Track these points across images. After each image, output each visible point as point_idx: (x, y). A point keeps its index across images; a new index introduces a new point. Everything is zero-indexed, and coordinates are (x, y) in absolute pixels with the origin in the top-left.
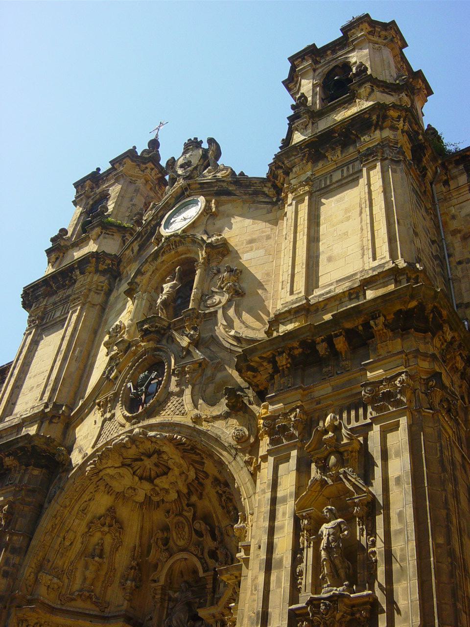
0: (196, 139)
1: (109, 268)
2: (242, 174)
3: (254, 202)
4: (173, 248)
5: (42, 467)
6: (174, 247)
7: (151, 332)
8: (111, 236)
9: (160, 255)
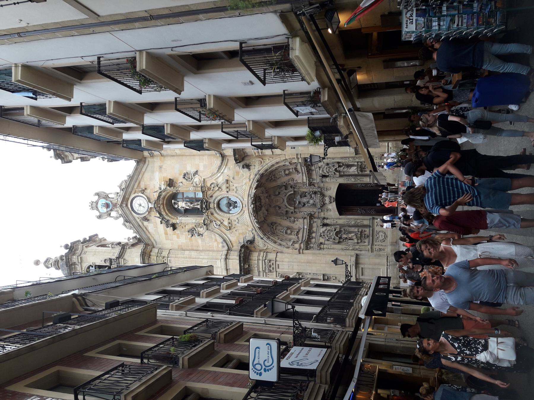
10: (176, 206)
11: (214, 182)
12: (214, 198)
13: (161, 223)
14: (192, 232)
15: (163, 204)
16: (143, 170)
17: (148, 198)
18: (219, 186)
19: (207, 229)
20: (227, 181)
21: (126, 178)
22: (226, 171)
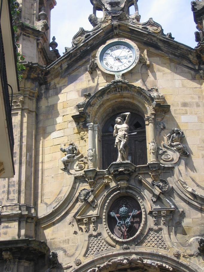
1: (38, 77)
3: (179, 64)
4: (119, 92)
5: (30, 260)
6: (120, 90)
7: (124, 174)
8: (28, 38)
10: (118, 120)
21: (165, 33)
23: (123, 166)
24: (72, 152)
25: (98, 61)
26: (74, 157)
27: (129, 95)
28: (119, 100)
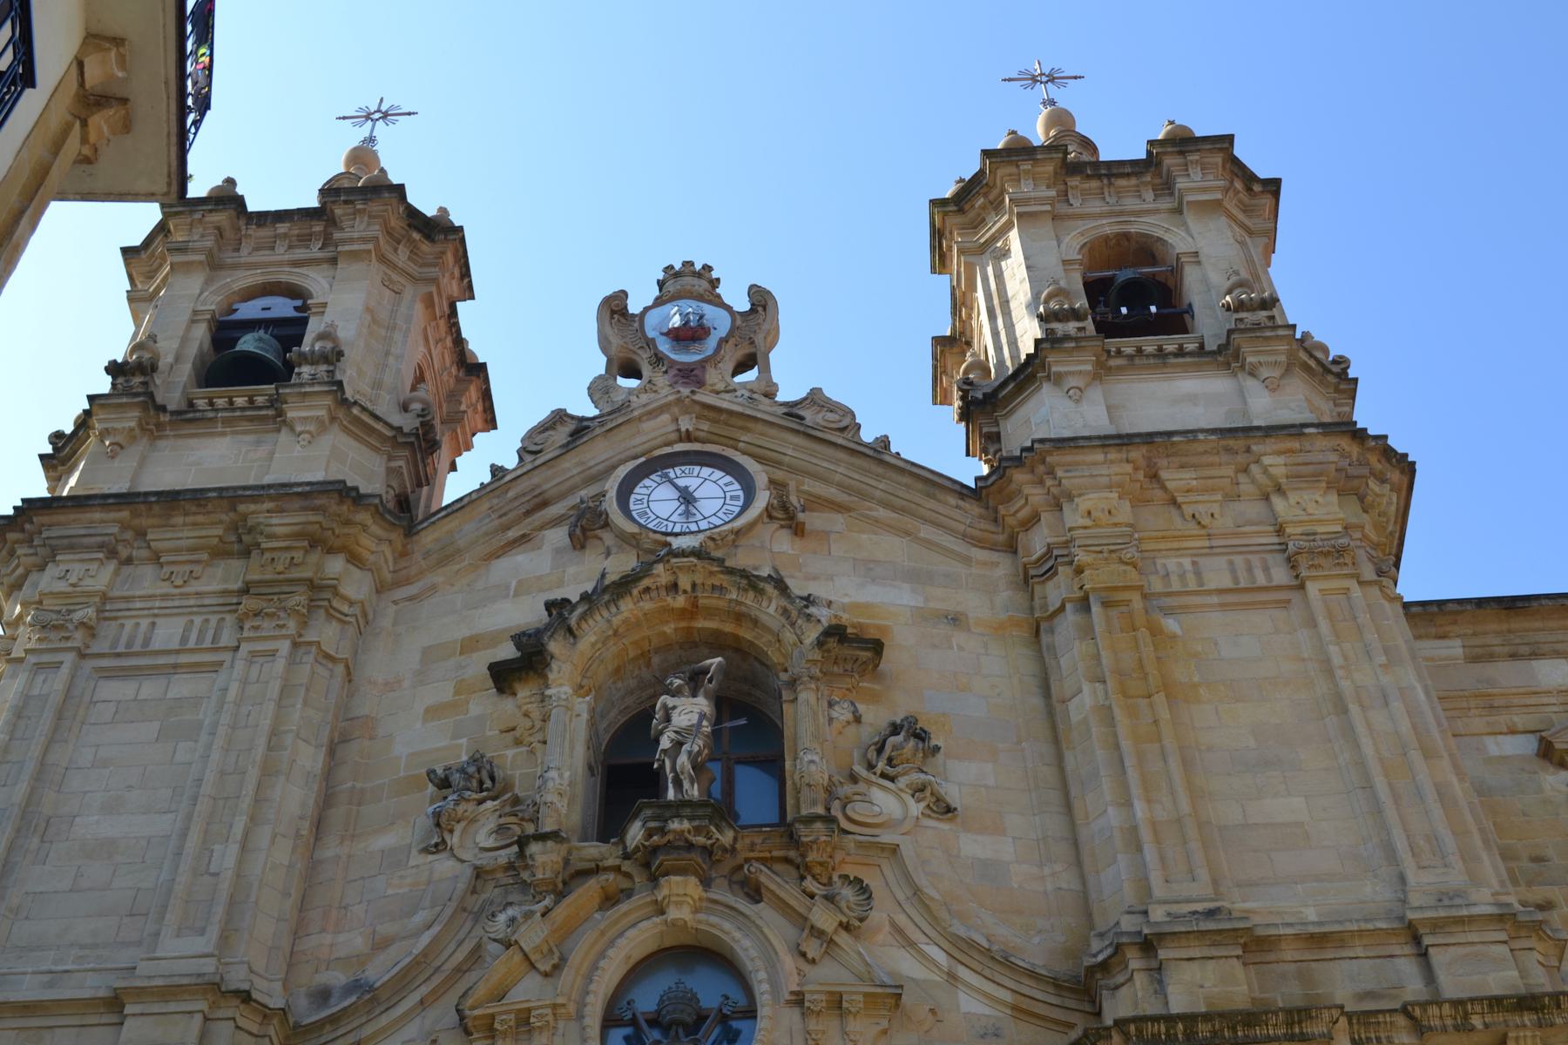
0: (708, 268)
2: (884, 442)
7: (690, 846)
9: (635, 592)
11: (877, 916)
12: (742, 904)
13: (549, 606)
14: (470, 781)
15: (693, 610)
16: (926, 532)
17: (738, 533)
18: (843, 938)
19: (479, 873)
20: (890, 998)
21: (867, 436)
22: (969, 1004)
23: (687, 811)
24: (475, 784)
25: (611, 505)
26: (480, 802)
27: (722, 604)
28: (683, 624)
